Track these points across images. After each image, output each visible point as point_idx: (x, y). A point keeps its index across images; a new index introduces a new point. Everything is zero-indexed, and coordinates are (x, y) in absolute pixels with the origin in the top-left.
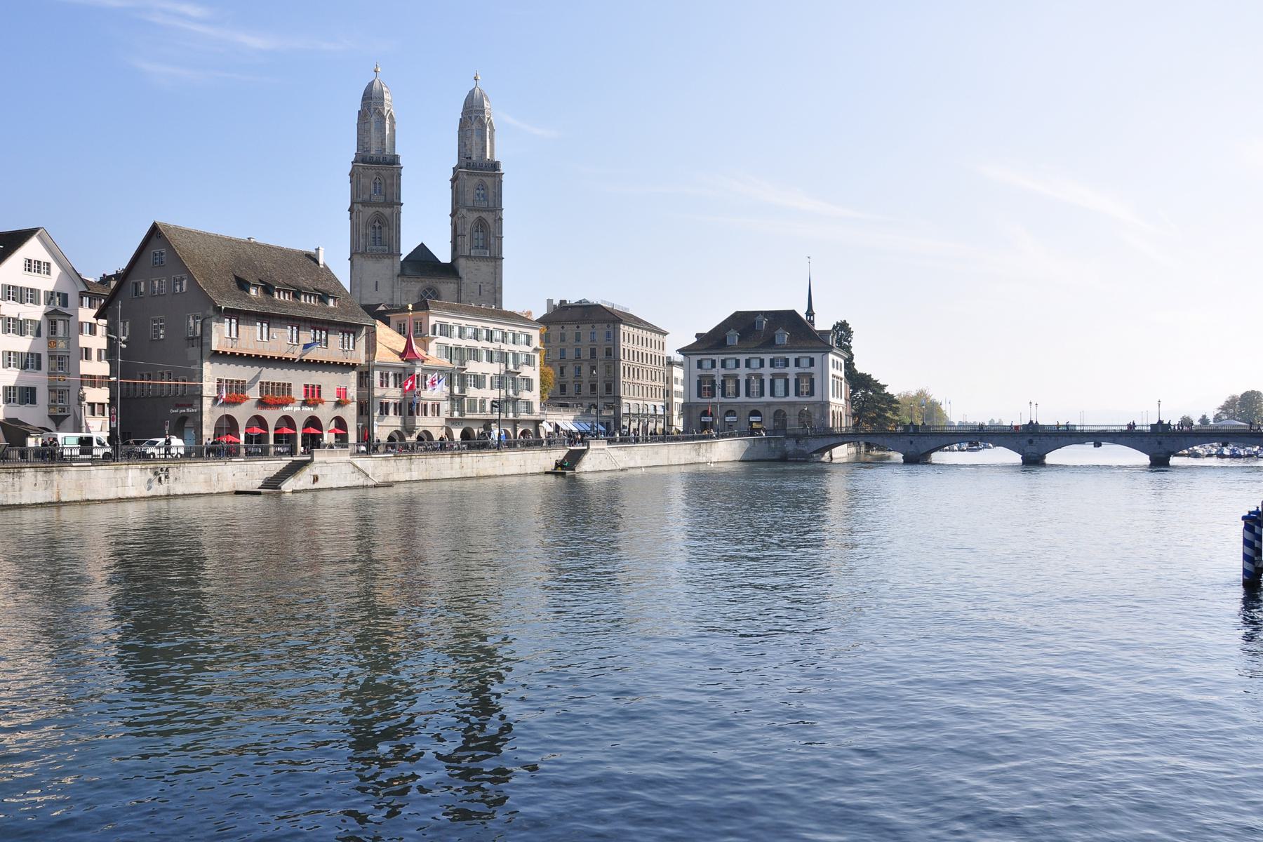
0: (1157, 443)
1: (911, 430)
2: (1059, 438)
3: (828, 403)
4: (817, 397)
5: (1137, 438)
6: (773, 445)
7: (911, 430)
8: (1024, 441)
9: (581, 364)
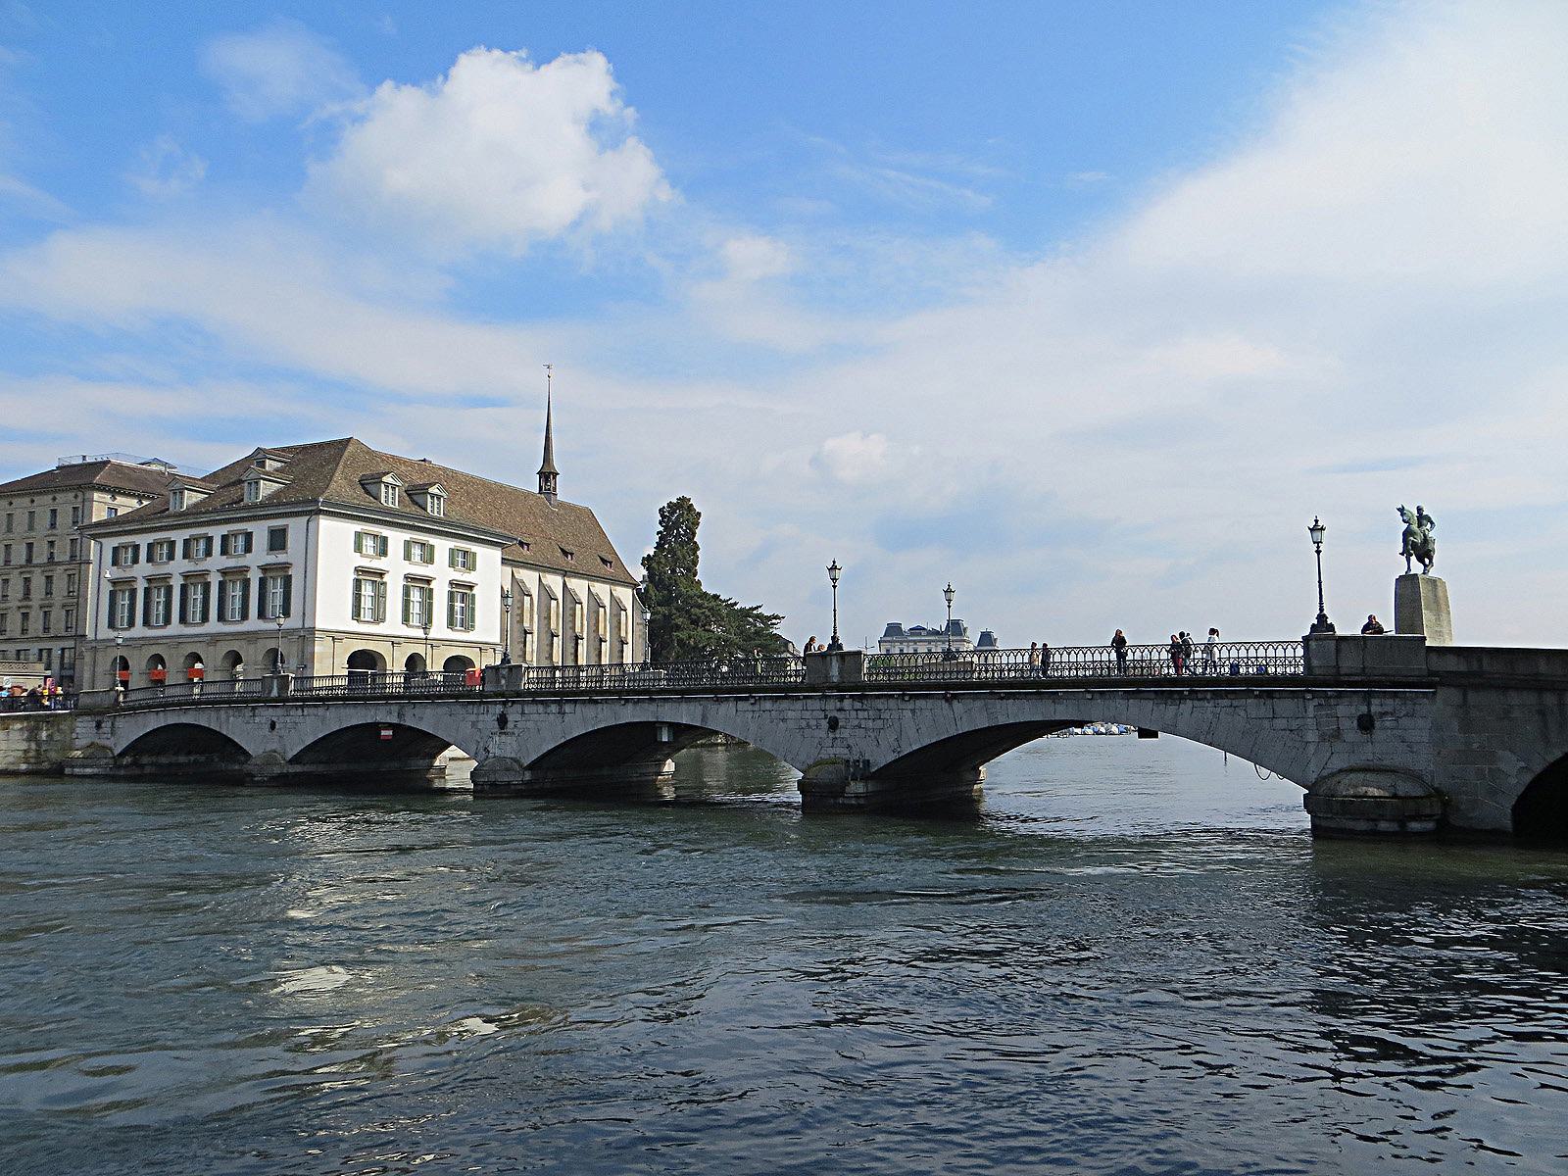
0: (825, 724)
1: (275, 693)
2: (568, 708)
3: (313, 630)
4: (292, 622)
5: (768, 705)
6: (44, 735)
7: (275, 693)
8: (488, 718)
9: (29, 572)
